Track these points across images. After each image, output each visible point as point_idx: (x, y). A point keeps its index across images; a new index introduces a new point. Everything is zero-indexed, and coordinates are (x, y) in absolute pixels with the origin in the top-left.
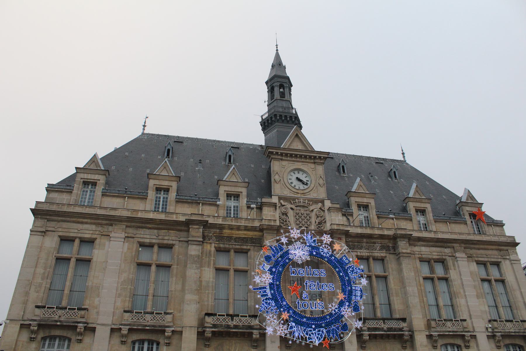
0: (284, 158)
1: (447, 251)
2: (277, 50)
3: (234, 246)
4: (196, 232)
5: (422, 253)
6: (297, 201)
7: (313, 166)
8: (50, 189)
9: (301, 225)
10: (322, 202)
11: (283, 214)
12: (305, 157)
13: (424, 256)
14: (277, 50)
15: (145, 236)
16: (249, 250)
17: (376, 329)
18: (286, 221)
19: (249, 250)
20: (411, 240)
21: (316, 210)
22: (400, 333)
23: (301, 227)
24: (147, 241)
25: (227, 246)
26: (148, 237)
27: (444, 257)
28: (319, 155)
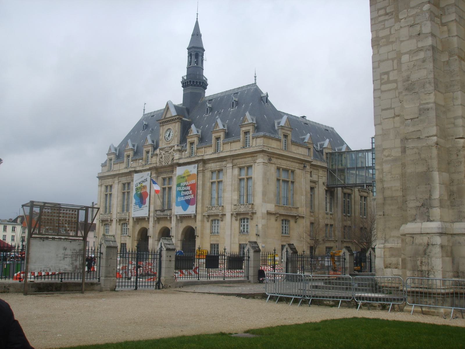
1: (224, 163)
2: (197, 19)
5: (212, 167)
8: (103, 165)
10: (174, 147)
13: (212, 169)
14: (197, 19)
27: (222, 168)
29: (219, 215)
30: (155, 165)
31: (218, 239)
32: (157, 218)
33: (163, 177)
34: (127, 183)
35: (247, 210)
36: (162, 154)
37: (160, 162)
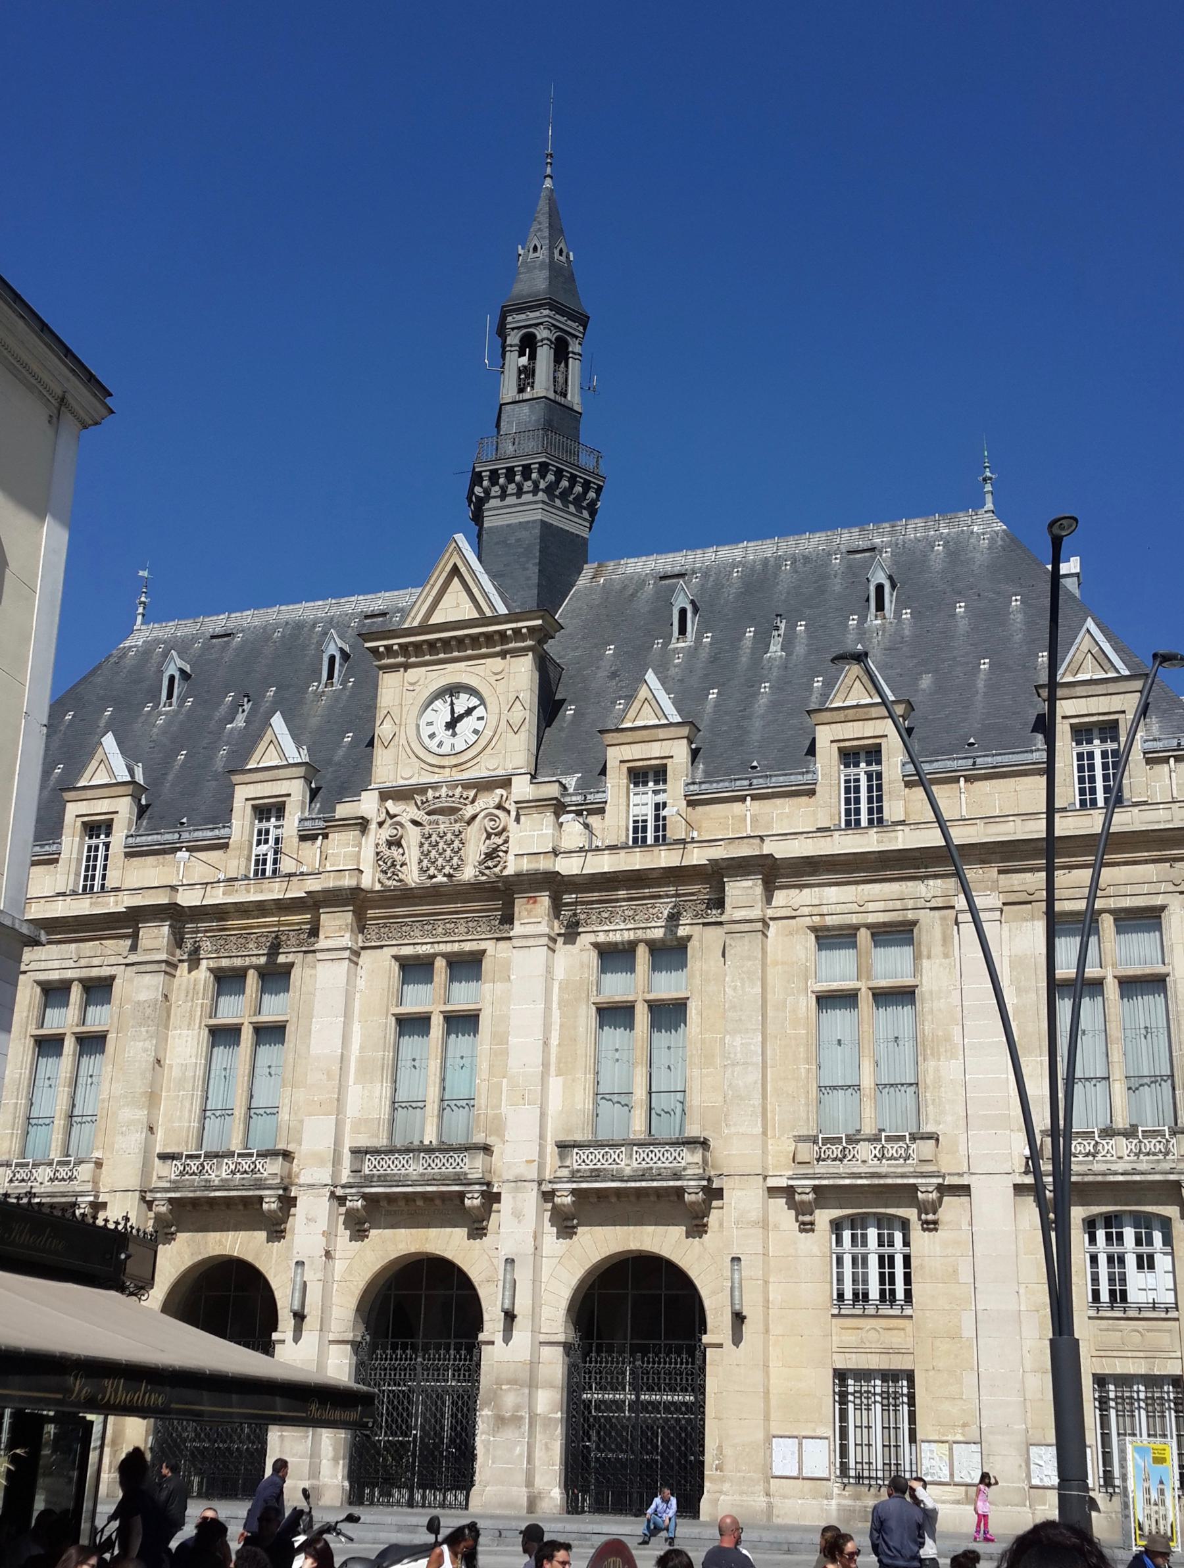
0: (413, 660)
3: (254, 959)
4: (156, 936)
5: (824, 909)
6: (430, 793)
7: (496, 663)
9: (432, 871)
11: (390, 844)
12: (475, 640)
13: (830, 921)
15: (50, 965)
16: (292, 965)
17: (596, 1174)
18: (393, 865)
19: (292, 965)
20: (773, 873)
21: (482, 814)
22: (671, 1183)
23: (434, 876)
24: (55, 976)
25: (238, 962)
26: (56, 964)
27: (910, 915)
28: (514, 625)
29: (915, 1187)
30: (348, 882)
31: (896, 1340)
32: (365, 1196)
33: (407, 951)
34: (80, 980)
35: (1167, 1166)
36: (404, 819)
37: (389, 867)
